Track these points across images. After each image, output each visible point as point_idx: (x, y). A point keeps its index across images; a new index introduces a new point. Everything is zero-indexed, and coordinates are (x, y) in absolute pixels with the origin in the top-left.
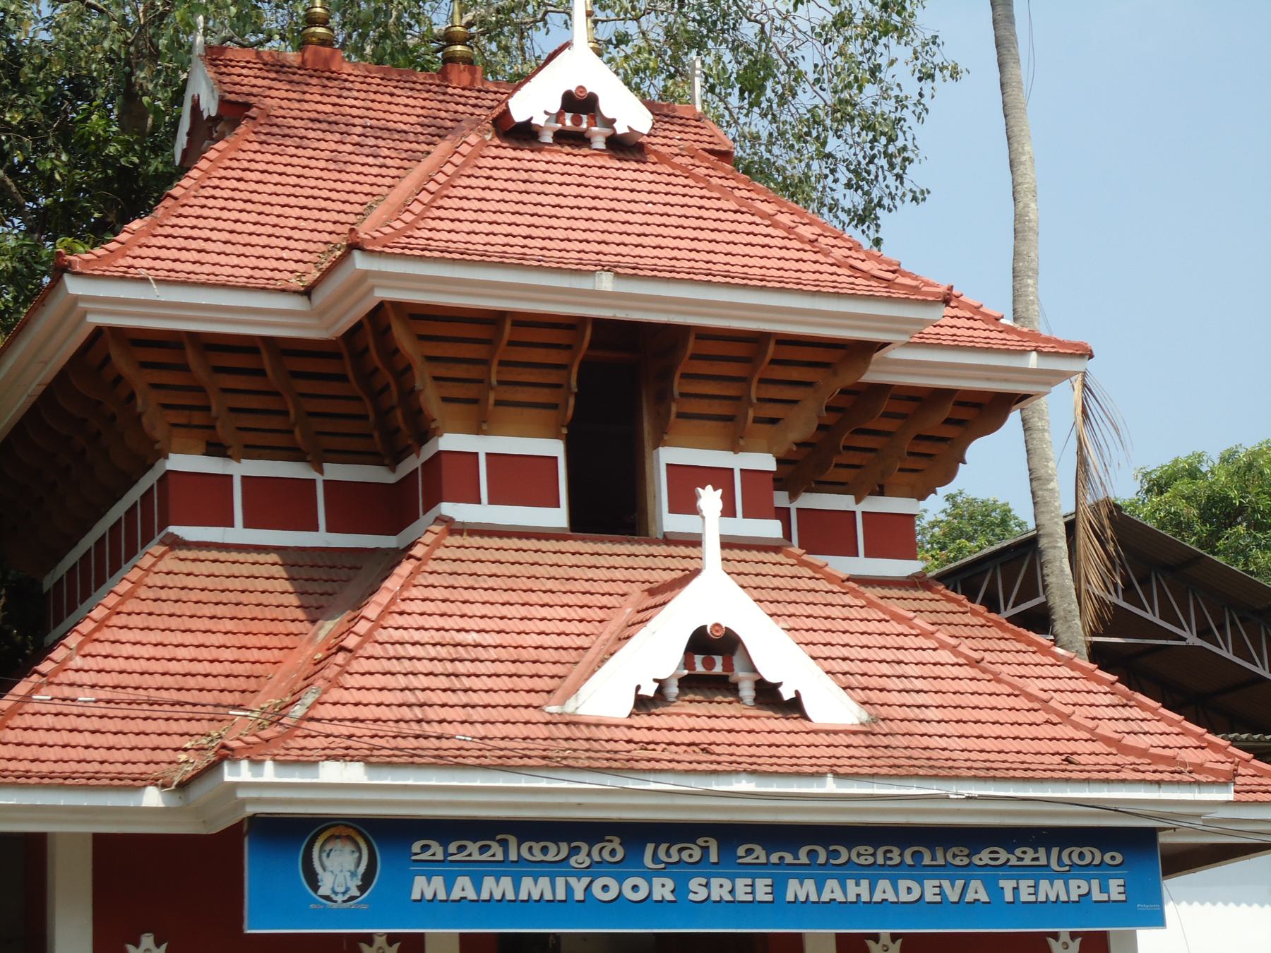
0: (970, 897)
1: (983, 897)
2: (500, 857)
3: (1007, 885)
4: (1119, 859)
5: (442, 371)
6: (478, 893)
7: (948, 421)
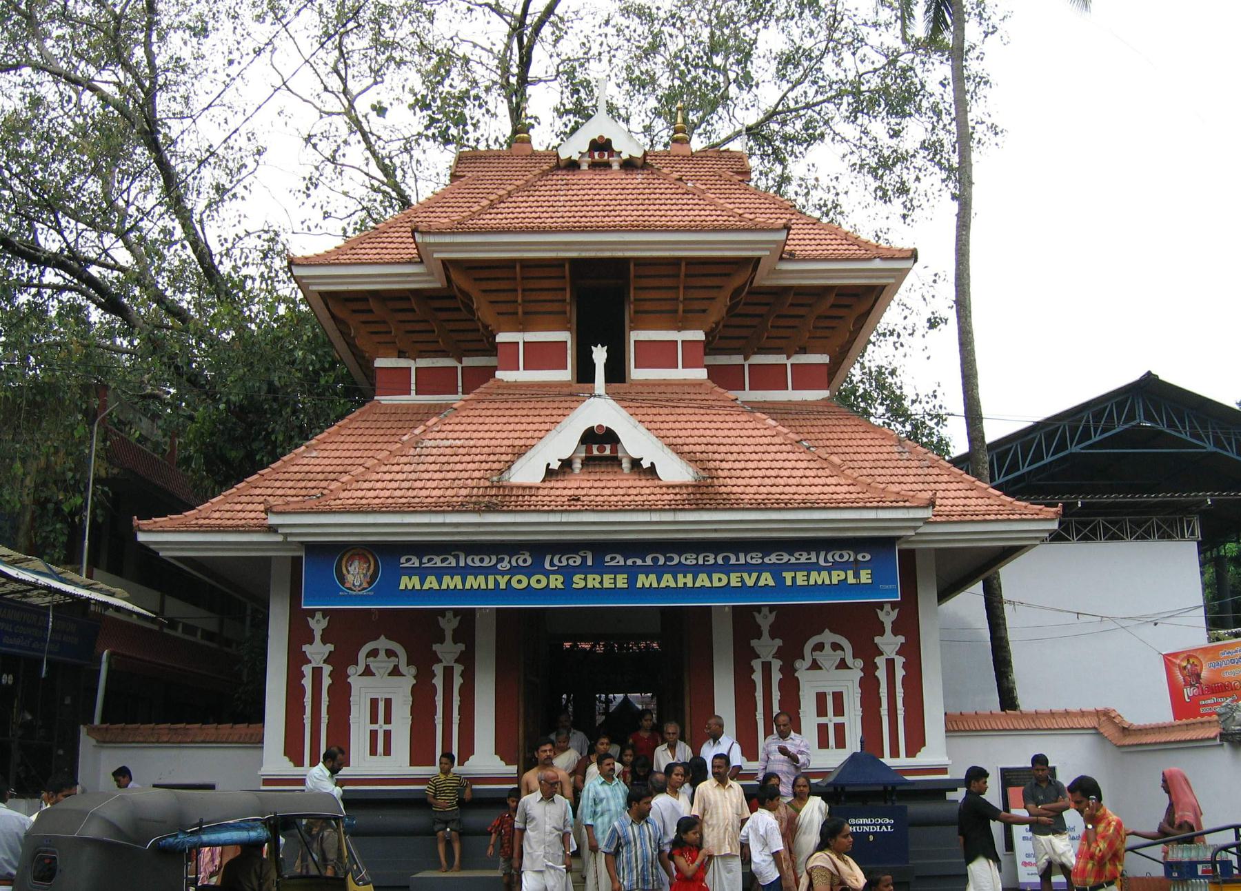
0: (761, 583)
1: (771, 583)
2: (454, 564)
3: (788, 576)
4: (868, 557)
5: (493, 297)
6: (440, 586)
7: (833, 306)
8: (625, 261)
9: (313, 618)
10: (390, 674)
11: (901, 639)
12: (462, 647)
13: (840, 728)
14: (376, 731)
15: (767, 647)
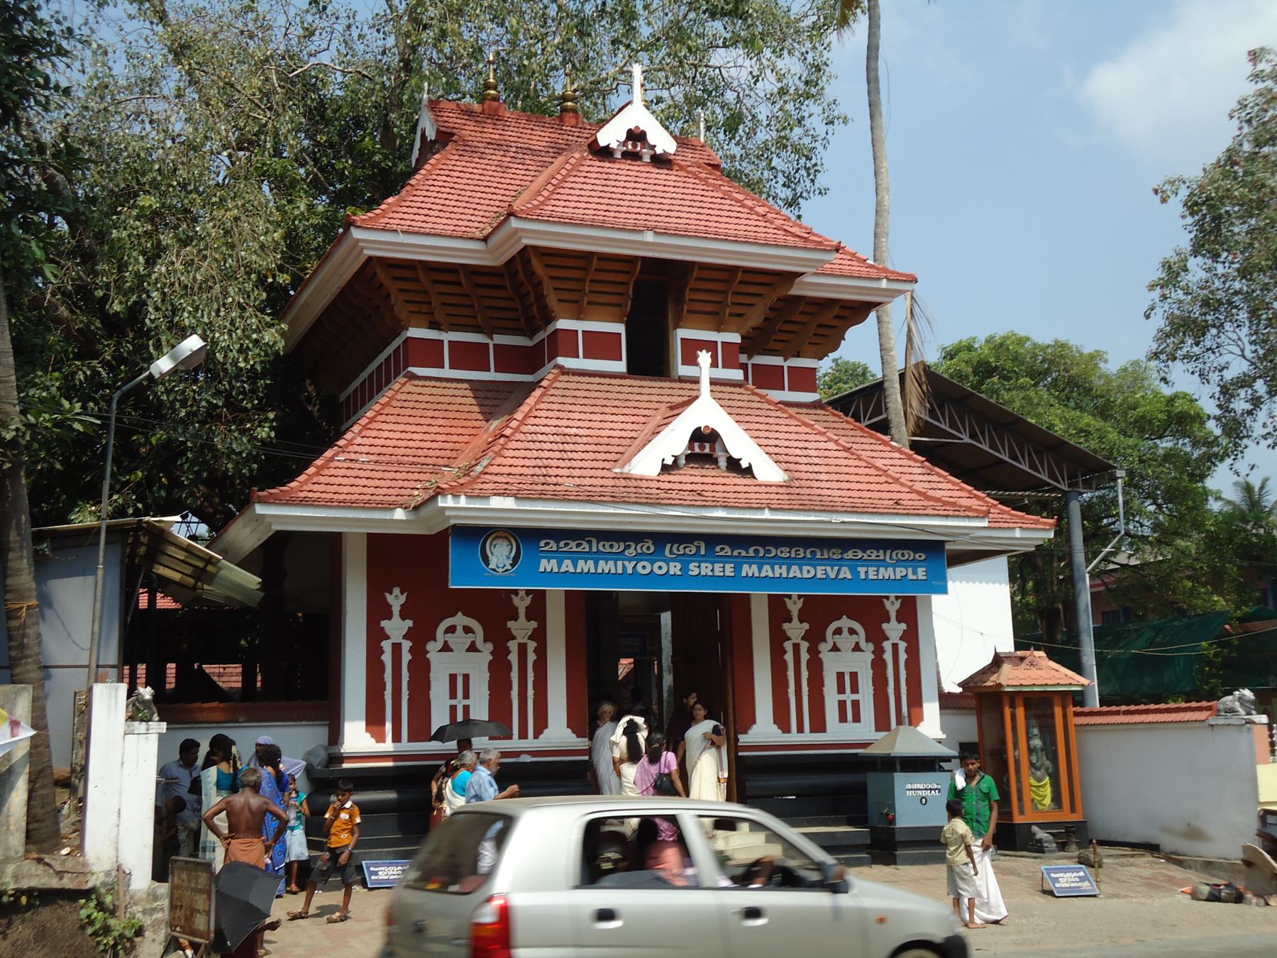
0: (841, 576)
1: (849, 576)
2: (587, 550)
3: (862, 570)
4: (923, 557)
5: (558, 284)
6: (575, 568)
7: (836, 317)
8: (691, 264)
9: (391, 593)
10: (468, 650)
11: (903, 626)
12: (534, 624)
13: (856, 704)
14: (845, 702)
15: (796, 630)
